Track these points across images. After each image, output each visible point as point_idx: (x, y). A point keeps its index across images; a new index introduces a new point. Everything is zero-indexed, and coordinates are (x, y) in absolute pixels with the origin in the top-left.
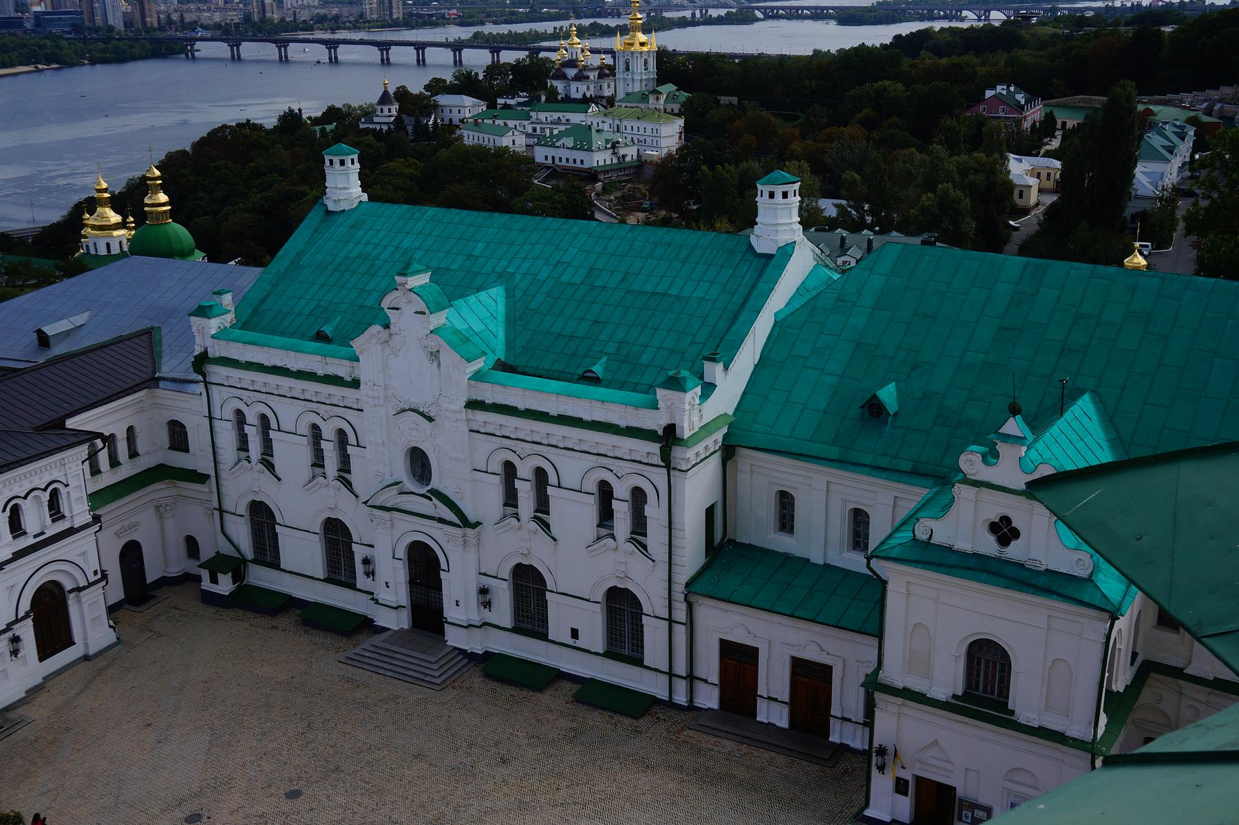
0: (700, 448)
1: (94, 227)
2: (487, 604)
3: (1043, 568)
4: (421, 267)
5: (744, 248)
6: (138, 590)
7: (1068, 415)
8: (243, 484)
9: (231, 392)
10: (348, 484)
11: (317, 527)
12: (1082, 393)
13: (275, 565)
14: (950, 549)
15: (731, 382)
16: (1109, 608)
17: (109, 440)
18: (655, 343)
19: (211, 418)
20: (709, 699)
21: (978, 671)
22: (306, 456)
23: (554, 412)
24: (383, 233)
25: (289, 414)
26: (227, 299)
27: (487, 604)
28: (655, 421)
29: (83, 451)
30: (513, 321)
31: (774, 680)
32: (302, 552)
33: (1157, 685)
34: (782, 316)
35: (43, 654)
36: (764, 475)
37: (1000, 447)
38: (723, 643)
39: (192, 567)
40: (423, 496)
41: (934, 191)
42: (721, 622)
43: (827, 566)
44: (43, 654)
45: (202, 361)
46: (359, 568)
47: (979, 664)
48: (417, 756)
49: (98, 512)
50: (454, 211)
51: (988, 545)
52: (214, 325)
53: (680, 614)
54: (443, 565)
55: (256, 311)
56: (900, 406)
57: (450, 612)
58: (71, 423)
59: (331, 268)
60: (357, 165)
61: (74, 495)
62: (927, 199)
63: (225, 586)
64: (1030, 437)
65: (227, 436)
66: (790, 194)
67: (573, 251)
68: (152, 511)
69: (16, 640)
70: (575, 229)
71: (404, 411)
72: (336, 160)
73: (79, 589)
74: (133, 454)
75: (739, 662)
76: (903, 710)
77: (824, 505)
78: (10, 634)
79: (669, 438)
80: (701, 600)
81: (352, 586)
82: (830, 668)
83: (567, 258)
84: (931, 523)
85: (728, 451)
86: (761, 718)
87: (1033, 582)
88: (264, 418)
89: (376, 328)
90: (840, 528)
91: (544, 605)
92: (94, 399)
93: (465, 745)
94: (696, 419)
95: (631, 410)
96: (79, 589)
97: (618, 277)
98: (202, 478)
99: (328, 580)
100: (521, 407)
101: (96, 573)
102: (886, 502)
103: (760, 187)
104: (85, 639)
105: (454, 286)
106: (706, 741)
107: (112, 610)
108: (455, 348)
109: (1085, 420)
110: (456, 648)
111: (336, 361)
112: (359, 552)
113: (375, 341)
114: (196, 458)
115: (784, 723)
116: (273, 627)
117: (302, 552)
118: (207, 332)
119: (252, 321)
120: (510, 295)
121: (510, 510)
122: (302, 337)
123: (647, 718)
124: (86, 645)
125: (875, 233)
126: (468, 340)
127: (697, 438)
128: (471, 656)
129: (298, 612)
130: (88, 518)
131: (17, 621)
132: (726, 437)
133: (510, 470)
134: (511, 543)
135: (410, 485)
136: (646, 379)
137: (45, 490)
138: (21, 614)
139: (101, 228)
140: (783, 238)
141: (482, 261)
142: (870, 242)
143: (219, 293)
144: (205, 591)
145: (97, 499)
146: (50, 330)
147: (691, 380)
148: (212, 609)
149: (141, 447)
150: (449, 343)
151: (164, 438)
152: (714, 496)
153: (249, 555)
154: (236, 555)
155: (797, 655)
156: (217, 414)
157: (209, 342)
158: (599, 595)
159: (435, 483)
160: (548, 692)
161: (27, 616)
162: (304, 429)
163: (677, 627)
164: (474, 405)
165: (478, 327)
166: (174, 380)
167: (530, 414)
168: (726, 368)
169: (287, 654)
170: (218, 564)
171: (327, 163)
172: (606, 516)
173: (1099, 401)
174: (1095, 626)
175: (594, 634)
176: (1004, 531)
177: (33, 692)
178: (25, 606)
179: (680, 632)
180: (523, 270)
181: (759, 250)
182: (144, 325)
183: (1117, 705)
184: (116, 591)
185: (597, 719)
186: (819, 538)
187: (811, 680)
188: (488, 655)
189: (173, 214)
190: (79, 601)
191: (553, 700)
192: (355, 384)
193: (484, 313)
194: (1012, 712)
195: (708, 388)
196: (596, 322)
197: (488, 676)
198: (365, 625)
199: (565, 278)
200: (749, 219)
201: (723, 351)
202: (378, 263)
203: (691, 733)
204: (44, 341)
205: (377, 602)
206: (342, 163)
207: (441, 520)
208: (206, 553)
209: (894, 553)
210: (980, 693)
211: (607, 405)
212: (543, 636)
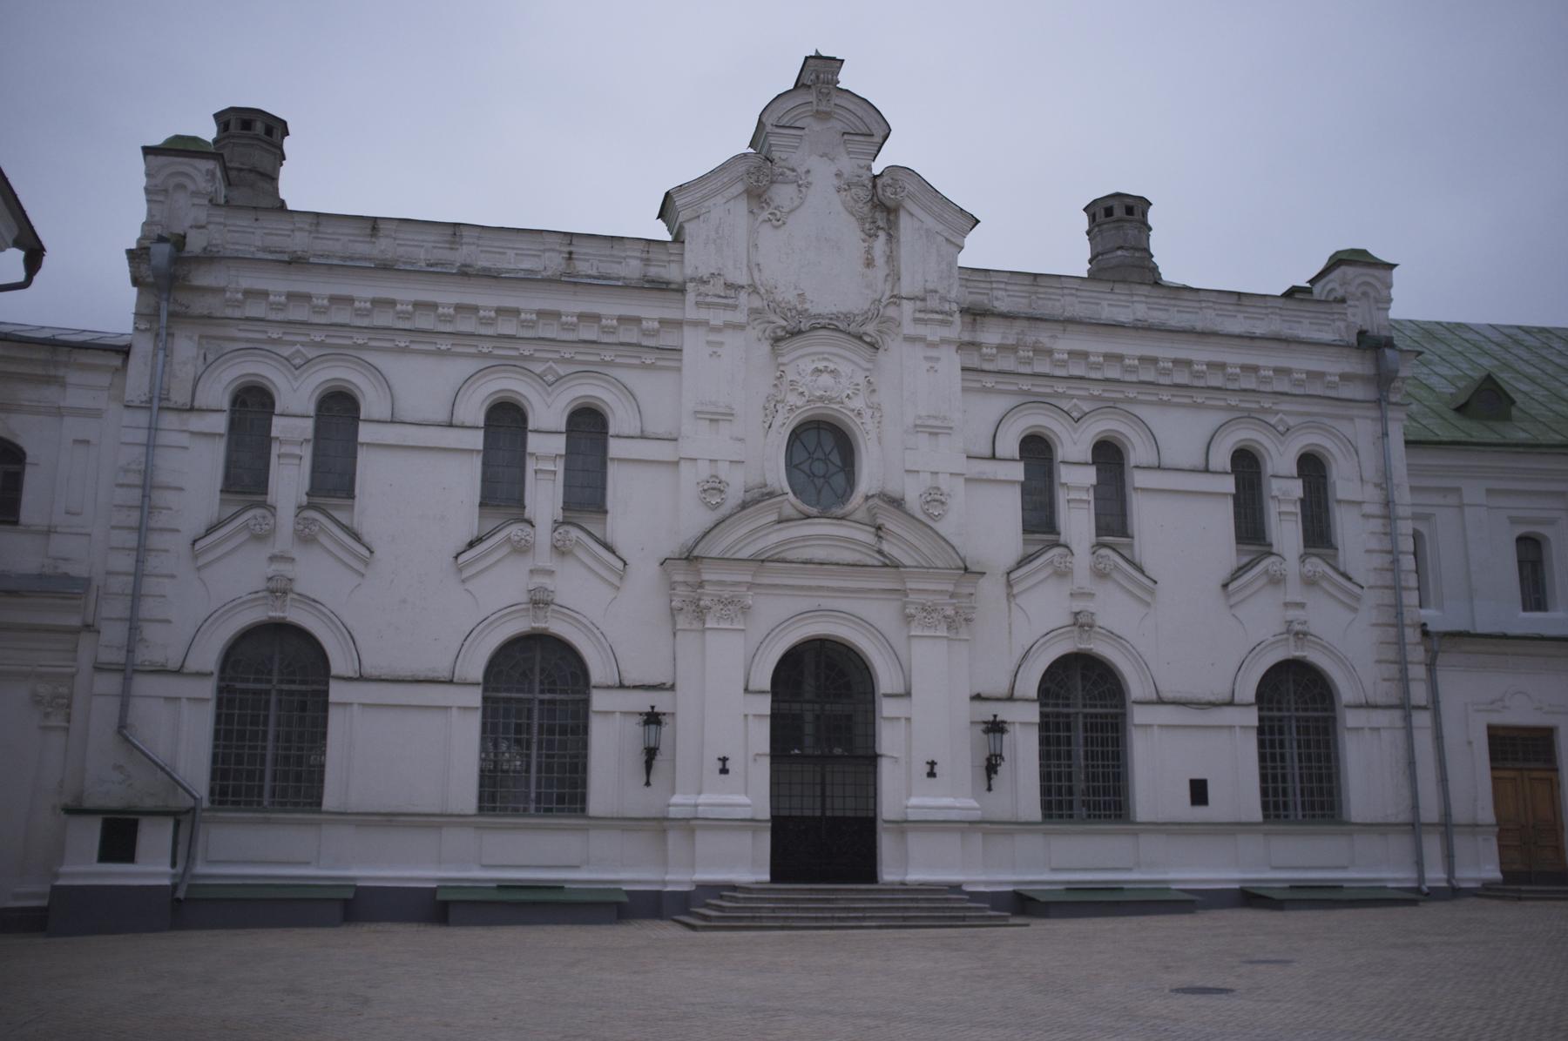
20: (1481, 864)
53: (1419, 694)
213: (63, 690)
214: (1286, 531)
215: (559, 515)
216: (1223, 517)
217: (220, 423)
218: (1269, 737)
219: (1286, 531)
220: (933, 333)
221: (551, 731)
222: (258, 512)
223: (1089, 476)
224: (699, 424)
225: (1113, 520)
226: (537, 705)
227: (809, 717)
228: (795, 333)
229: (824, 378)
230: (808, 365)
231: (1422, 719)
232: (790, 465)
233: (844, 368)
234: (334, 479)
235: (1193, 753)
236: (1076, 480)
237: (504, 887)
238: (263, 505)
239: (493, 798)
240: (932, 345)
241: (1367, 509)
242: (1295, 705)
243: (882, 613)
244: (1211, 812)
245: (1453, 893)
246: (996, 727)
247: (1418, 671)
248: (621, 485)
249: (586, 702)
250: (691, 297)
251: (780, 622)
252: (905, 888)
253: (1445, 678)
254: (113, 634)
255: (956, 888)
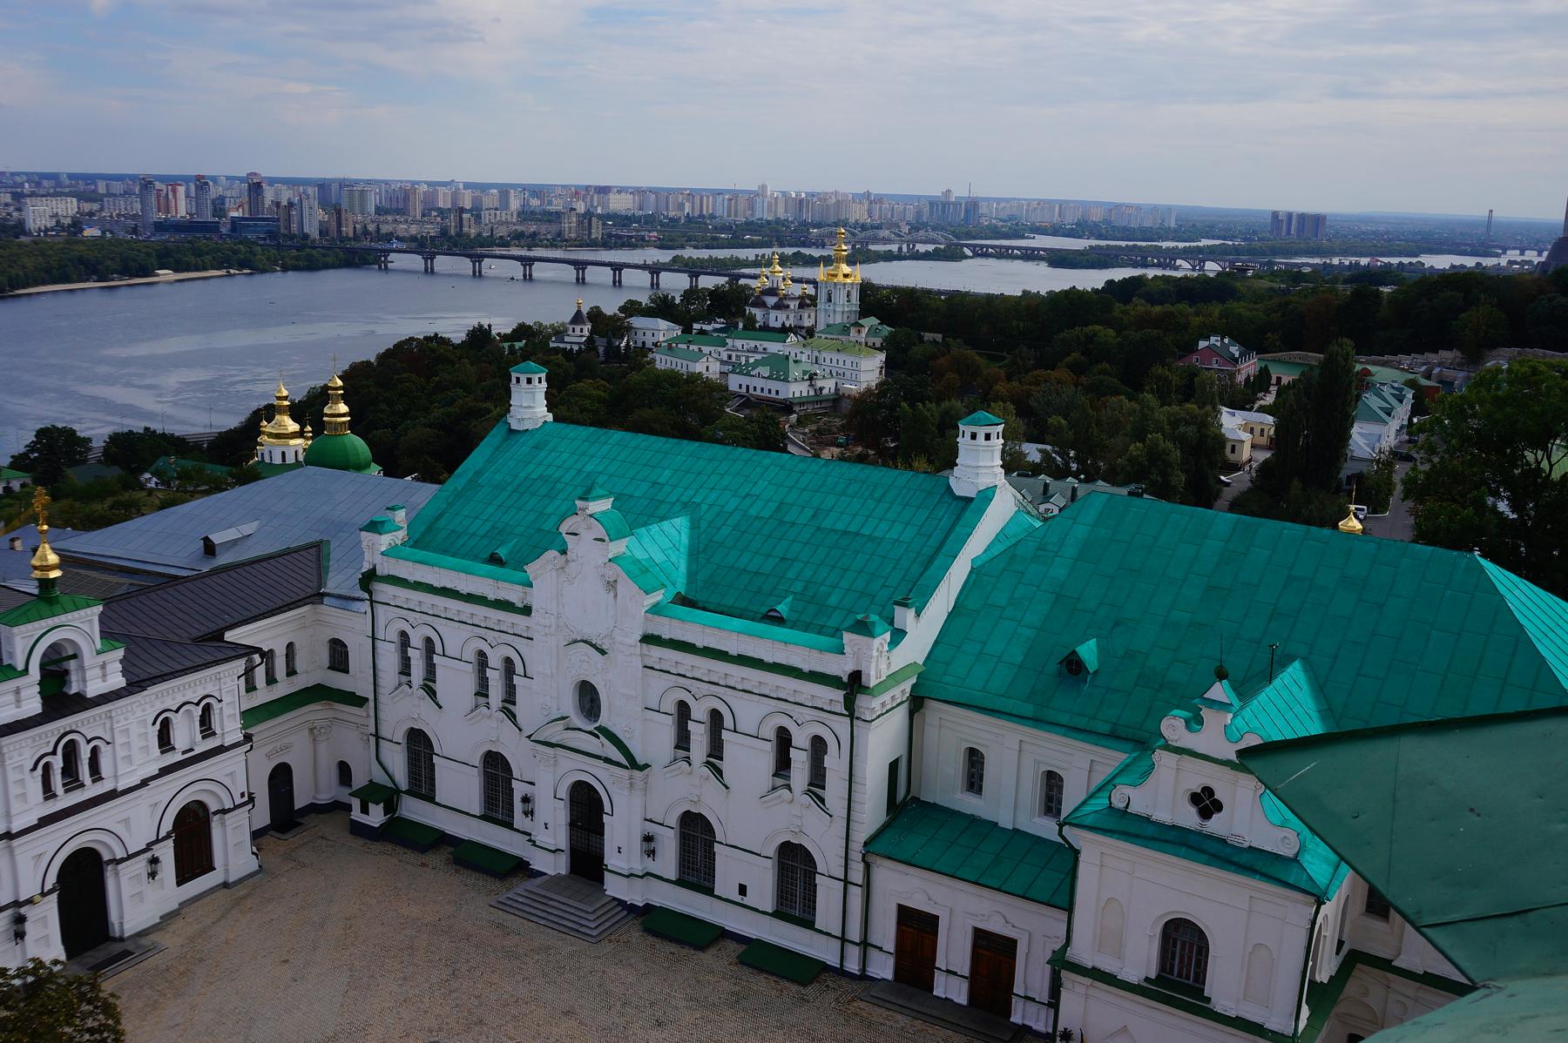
0: (886, 697)
1: (270, 435)
2: (651, 853)
3: (1246, 845)
4: (601, 492)
5: (943, 490)
6: (286, 815)
7: (1277, 682)
8: (402, 710)
9: (398, 612)
10: (512, 716)
11: (477, 760)
12: (1291, 659)
13: (430, 798)
14: (1147, 819)
15: (923, 628)
16: (1315, 891)
17: (268, 656)
18: (845, 584)
19: (374, 638)
20: (883, 968)
21: (1174, 954)
22: (470, 683)
23: (733, 652)
24: (565, 456)
25: (455, 639)
26: (401, 515)
27: (651, 853)
28: (840, 667)
29: (239, 665)
30: (697, 553)
31: (953, 952)
32: (459, 786)
33: (1363, 976)
34: (979, 563)
35: (182, 879)
36: (953, 730)
37: (1205, 713)
38: (902, 910)
39: (343, 795)
40: (590, 733)
41: (1143, 441)
42: (901, 886)
43: (1016, 831)
44: (182, 879)
45: (369, 579)
46: (518, 806)
47: (1175, 946)
48: (567, 1013)
49: (249, 731)
50: (642, 436)
51: (1189, 817)
52: (385, 541)
53: (857, 875)
54: (607, 808)
55: (429, 529)
56: (1100, 664)
57: (611, 860)
58: (229, 636)
59: (509, 489)
60: (544, 384)
61: (227, 712)
62: (1136, 449)
63: (376, 816)
64: (1237, 703)
65: (389, 659)
66: (993, 436)
67: (762, 484)
68: (306, 732)
69: (154, 861)
70: (767, 461)
71: (575, 641)
72: (523, 379)
73: (224, 811)
74: (291, 672)
75: (917, 929)
76: (1092, 991)
77: (1017, 766)
78: (148, 855)
79: (854, 685)
80: (879, 861)
81: (509, 825)
82: (1015, 942)
83: (756, 491)
84: (1129, 791)
85: (916, 703)
86: (938, 991)
87: (1236, 859)
88: (429, 641)
89: (552, 554)
90: (1032, 791)
91: (711, 856)
92: (256, 612)
93: (618, 1004)
94: (883, 667)
95: (815, 654)
96: (224, 811)
97: (809, 513)
98: (360, 701)
99: (483, 817)
100: (700, 644)
101: (242, 795)
102: (1083, 765)
103: (962, 428)
104: (226, 865)
105: (636, 513)
106: (878, 1014)
107: (256, 835)
108: (633, 578)
109: (1295, 690)
110: (615, 899)
111: (507, 585)
112: (519, 790)
113: (550, 567)
114: (356, 680)
115: (962, 999)
116: (423, 865)
117: (459, 786)
118: (378, 549)
119: (424, 539)
120: (694, 526)
121: (682, 753)
122: (475, 558)
123: (816, 985)
124: (227, 871)
125: (1080, 481)
126: (647, 570)
127: (884, 686)
128: (631, 909)
129: (450, 849)
130: (239, 737)
131: (158, 841)
132: (914, 687)
133: (683, 710)
134: (677, 789)
135: (578, 721)
136: (833, 623)
137: (197, 704)
138: (162, 834)
139: (278, 436)
140: (984, 482)
141: (668, 489)
142: (1074, 490)
143: (392, 509)
144: (353, 819)
145: (252, 716)
146: (217, 538)
147: (880, 625)
148: (360, 841)
149: (300, 663)
150: (628, 573)
151: (324, 657)
152: (900, 750)
153: (403, 781)
154: (390, 785)
155: (980, 926)
156: (380, 634)
157: (378, 559)
158: (771, 851)
159: (604, 720)
160: (712, 951)
161: (168, 836)
162: (470, 655)
163: (852, 889)
164: (649, 639)
165: (659, 557)
166: (339, 597)
167: (709, 652)
168: (918, 614)
169: (434, 893)
170: (372, 792)
171: (514, 380)
172: (783, 764)
173: (1310, 669)
174: (1297, 910)
175: (764, 892)
176: (1206, 803)
177: (168, 918)
178: (167, 825)
179: (856, 894)
180: (710, 500)
181: (958, 493)
182: (314, 537)
183: (1320, 996)
184: (262, 815)
185: (761, 984)
186: (1009, 801)
187: (994, 953)
188: (649, 908)
189: (352, 426)
190: (223, 824)
191: (716, 960)
192: (527, 611)
193: (666, 543)
194: (1208, 1000)
195: (898, 635)
196: (783, 559)
197: (649, 931)
198: (520, 868)
199: (753, 512)
200: (948, 459)
201: (915, 595)
202: (559, 486)
203: (862, 1005)
204: (210, 549)
205: (534, 843)
206: (529, 381)
207: (608, 760)
208: (359, 781)
209: (1088, 821)
210: (1175, 977)
211: (790, 647)
212: (709, 891)
235: (745, 872)
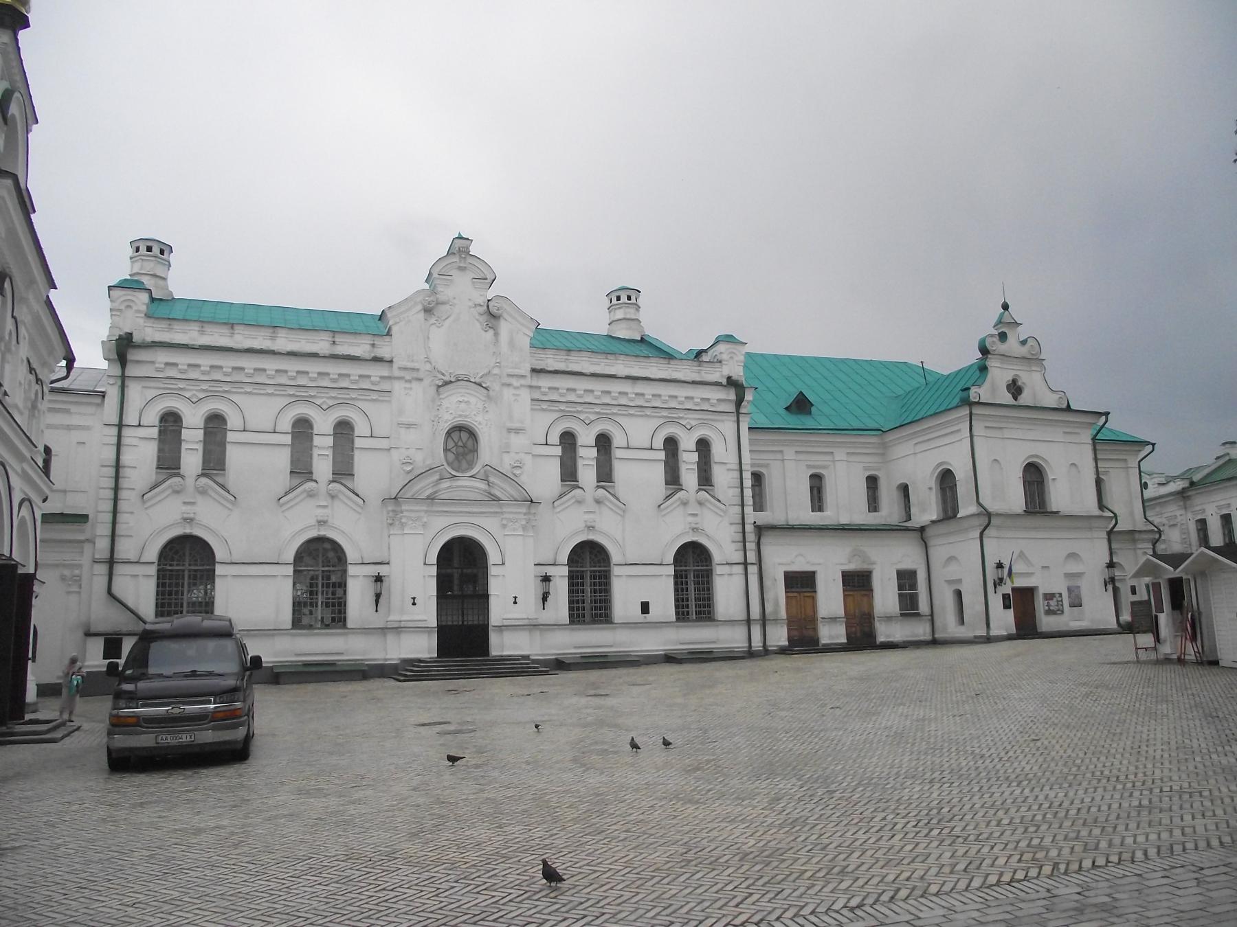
20: (779, 636)
31: (830, 599)
53: (752, 557)
86: (824, 640)
156: (131, 418)
175: (664, 605)
213: (77, 572)
214: (689, 477)
215: (331, 477)
216: (660, 470)
217: (154, 432)
218: (680, 580)
219: (689, 477)
220: (515, 382)
221: (328, 587)
222: (176, 480)
223: (594, 452)
224: (400, 430)
225: (605, 474)
226: (321, 575)
227: (456, 576)
228: (446, 383)
229: (460, 406)
230: (455, 399)
231: (753, 570)
232: (446, 450)
233: (473, 400)
234: (214, 462)
236: (587, 455)
237: (307, 664)
238: (178, 475)
239: (300, 620)
240: (516, 388)
241: (729, 466)
242: (693, 563)
243: (491, 523)
244: (651, 617)
245: (766, 652)
246: (546, 579)
247: (751, 546)
248: (362, 463)
249: (345, 571)
250: (395, 366)
251: (444, 528)
252: (502, 659)
253: (766, 550)
254: (103, 544)
255: (527, 657)
